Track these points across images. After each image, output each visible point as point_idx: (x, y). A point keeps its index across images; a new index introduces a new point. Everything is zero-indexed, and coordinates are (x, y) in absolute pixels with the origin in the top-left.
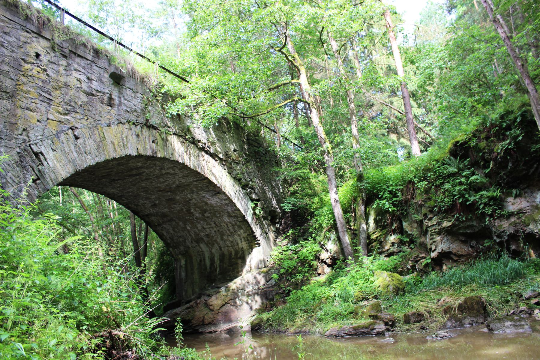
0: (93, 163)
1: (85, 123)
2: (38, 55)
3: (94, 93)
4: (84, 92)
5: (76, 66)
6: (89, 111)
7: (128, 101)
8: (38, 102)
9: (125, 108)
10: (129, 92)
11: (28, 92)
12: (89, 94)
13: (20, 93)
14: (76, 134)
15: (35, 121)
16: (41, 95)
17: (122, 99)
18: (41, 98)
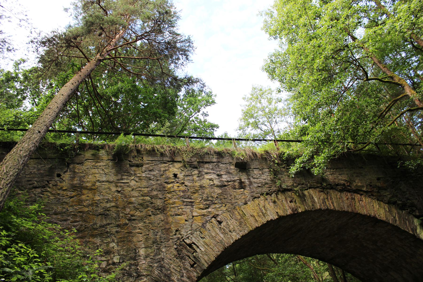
0: (238, 237)
1: (224, 209)
2: (175, 176)
3: (226, 184)
4: (217, 186)
5: (206, 171)
6: (225, 199)
7: (257, 178)
8: (183, 207)
9: (256, 185)
10: (256, 172)
11: (174, 203)
12: (222, 186)
13: (169, 206)
14: (219, 219)
15: (184, 221)
16: (184, 202)
17: (252, 179)
18: (185, 204)
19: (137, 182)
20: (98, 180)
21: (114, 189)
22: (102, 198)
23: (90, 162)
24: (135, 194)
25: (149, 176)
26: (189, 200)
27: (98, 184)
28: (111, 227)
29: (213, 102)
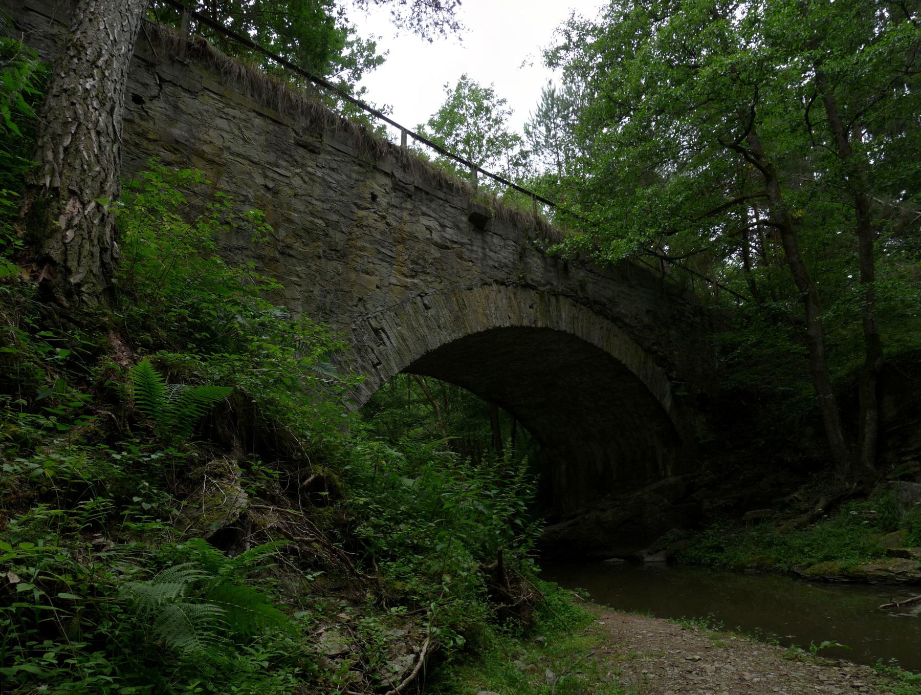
0: (449, 339)
1: (438, 287)
2: (374, 197)
3: (449, 244)
4: (436, 244)
5: (424, 209)
6: (443, 270)
7: (495, 252)
8: (376, 261)
9: (491, 263)
10: (496, 240)
11: (363, 249)
12: (442, 247)
13: (353, 250)
14: (426, 302)
15: (374, 287)
16: (379, 252)
17: (488, 250)
18: (380, 256)
19: (305, 182)
20: (229, 148)
21: (260, 180)
22: (235, 189)
23: (213, 98)
24: (299, 205)
25: (330, 179)
26: (390, 253)
27: (226, 155)
28: (246, 256)
29: (380, 60)
